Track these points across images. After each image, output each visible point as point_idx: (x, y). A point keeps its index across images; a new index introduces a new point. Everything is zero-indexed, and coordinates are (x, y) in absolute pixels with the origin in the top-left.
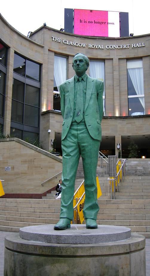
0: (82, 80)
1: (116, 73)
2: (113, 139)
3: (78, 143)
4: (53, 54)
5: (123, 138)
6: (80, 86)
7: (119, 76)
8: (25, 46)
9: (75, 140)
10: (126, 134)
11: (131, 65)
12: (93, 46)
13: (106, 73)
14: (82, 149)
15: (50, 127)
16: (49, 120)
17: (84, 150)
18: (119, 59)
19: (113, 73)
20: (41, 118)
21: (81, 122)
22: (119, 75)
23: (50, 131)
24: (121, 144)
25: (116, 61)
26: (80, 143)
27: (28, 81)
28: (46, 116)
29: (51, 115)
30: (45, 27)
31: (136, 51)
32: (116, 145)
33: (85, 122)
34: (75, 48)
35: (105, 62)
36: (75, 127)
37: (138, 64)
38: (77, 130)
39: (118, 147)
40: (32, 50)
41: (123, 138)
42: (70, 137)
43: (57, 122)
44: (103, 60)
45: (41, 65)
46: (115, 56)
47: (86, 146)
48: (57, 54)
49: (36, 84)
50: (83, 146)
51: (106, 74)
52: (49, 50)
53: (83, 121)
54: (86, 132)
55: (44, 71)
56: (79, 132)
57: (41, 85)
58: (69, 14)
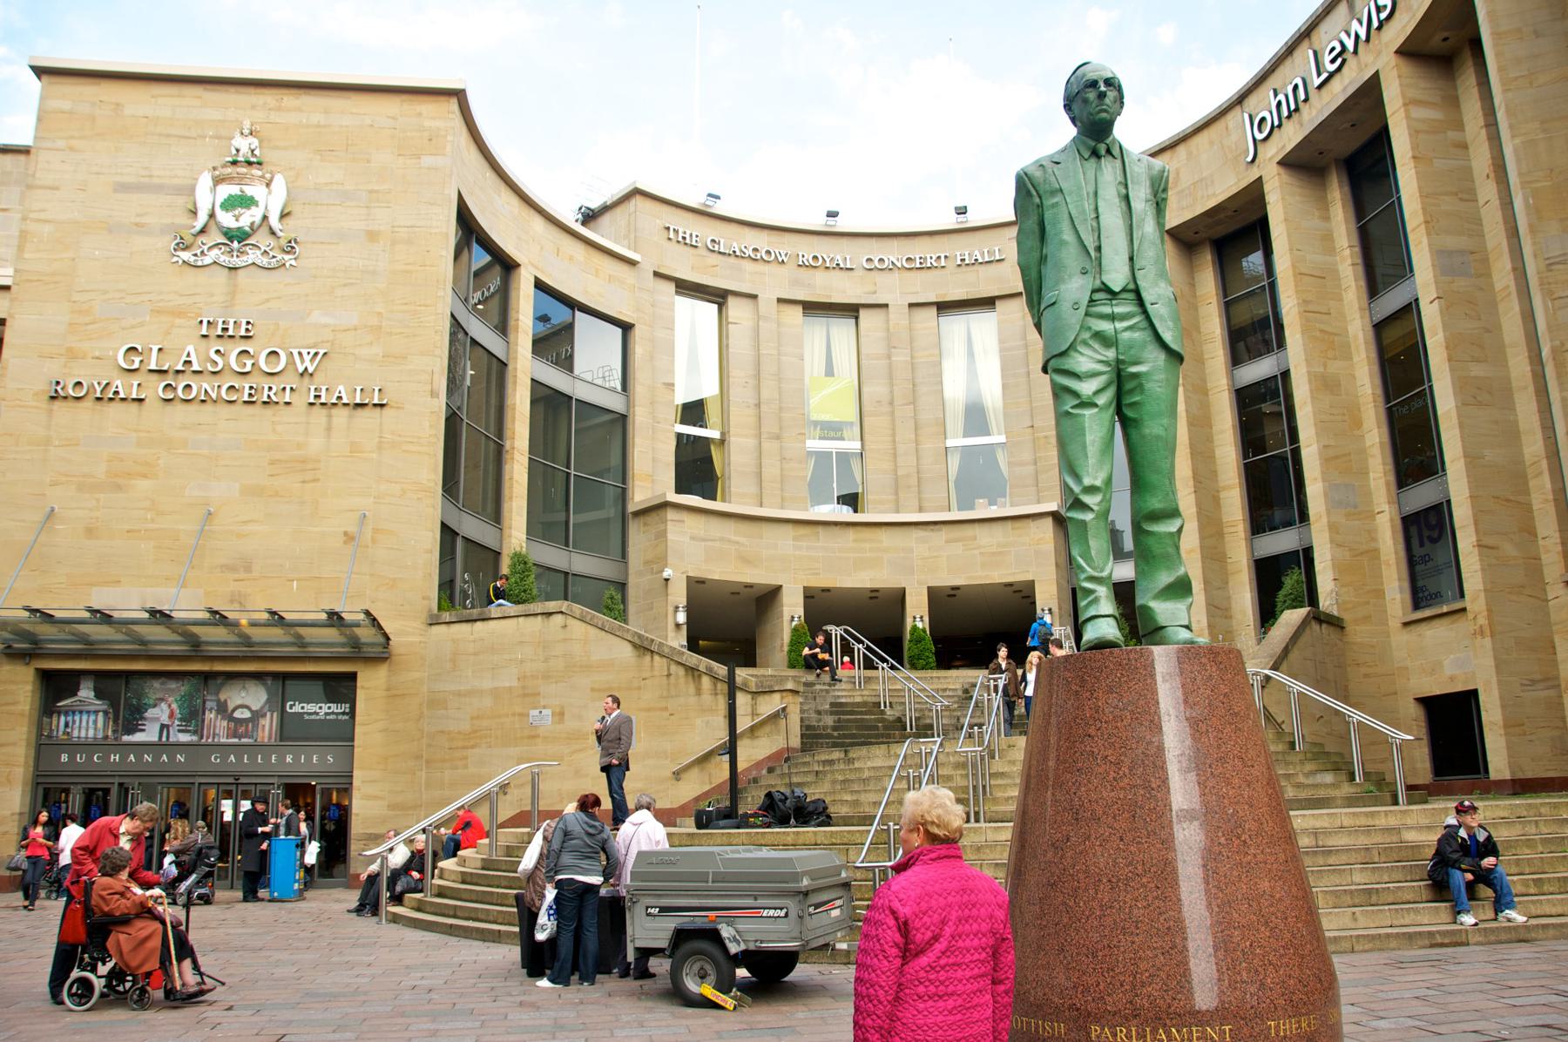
0: (1109, 151)
1: (901, 357)
2: (899, 597)
3: (1118, 361)
4: (671, 287)
5: (933, 593)
6: (1109, 171)
8: (571, 258)
9: (1111, 354)
11: (956, 325)
12: (815, 258)
13: (863, 357)
14: (1128, 386)
15: (670, 560)
16: (665, 531)
17: (1140, 388)
18: (911, 305)
19: (889, 357)
21: (1124, 290)
23: (667, 573)
24: (926, 619)
25: (898, 314)
26: (1123, 362)
28: (653, 518)
29: (671, 514)
31: (970, 275)
33: (1137, 292)
34: (748, 265)
35: (857, 318)
36: (1107, 310)
37: (983, 325)
38: (1112, 318)
40: (597, 276)
41: (933, 593)
42: (1085, 343)
43: (693, 538)
44: (851, 311)
45: (626, 328)
46: (895, 291)
47: (1146, 373)
48: (685, 288)
50: (1136, 376)
51: (863, 362)
52: (656, 274)
53: (1132, 286)
54: (1144, 324)
55: (639, 350)
56: (1120, 325)
57: (629, 403)
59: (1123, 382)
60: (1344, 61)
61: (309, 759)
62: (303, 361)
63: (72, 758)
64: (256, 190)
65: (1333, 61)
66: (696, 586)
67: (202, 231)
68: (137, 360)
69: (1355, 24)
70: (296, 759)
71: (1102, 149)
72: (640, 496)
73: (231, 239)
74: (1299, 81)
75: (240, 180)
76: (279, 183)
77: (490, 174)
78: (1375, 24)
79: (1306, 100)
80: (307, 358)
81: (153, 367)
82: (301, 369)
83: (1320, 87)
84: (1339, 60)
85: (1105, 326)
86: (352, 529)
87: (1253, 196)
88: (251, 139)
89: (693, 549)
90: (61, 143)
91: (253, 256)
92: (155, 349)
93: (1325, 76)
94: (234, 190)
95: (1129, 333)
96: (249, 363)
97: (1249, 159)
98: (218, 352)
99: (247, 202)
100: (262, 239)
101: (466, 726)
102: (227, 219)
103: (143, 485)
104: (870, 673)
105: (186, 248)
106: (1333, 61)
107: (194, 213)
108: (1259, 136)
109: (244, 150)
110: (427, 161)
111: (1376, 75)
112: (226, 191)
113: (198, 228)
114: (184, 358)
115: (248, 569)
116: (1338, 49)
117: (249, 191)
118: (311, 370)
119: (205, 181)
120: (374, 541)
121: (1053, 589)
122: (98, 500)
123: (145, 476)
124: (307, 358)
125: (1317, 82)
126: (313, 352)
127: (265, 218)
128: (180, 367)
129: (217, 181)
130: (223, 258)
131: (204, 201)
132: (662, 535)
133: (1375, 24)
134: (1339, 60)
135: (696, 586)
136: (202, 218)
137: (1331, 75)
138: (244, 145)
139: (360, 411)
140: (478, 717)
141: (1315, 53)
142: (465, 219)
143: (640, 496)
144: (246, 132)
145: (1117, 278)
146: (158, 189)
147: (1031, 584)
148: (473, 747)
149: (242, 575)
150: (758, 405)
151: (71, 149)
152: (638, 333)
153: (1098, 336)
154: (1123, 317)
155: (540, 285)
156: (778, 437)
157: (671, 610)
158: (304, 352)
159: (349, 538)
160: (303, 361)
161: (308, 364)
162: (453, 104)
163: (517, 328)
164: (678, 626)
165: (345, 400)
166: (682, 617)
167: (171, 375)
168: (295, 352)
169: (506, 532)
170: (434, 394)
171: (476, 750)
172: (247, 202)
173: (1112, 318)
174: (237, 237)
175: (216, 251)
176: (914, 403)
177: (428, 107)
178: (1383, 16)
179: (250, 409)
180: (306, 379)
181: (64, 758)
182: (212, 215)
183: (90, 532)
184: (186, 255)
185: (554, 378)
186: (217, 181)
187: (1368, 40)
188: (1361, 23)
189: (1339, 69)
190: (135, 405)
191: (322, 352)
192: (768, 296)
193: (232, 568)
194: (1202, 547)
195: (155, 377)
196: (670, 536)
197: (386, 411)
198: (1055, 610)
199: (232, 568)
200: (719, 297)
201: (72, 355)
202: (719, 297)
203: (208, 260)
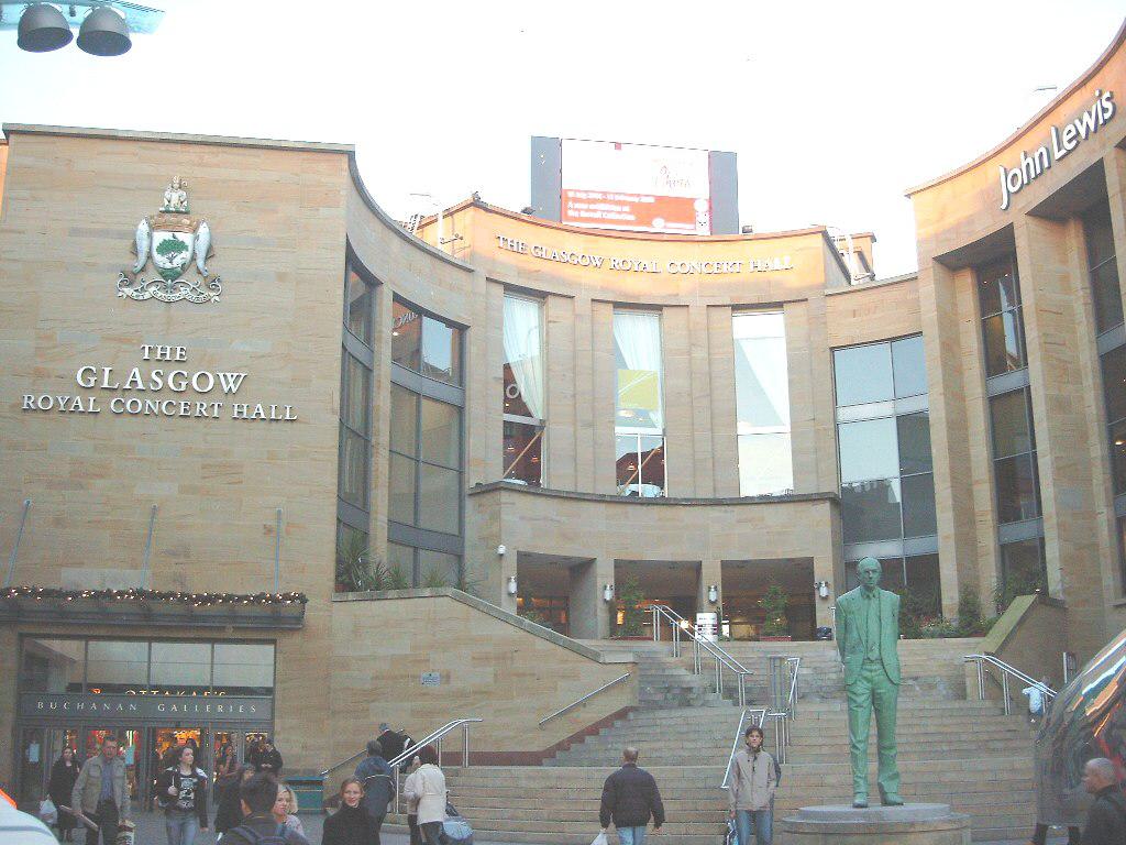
5: (726, 565)
7: (710, 364)
10: (736, 555)
20: (469, 504)
22: (710, 360)
23: (502, 550)
24: (720, 588)
27: (429, 386)
28: (487, 499)
29: (505, 497)
30: (476, 203)
32: (705, 590)
37: (774, 322)
39: (713, 596)
41: (726, 565)
48: (510, 289)
49: (450, 393)
58: (546, 155)
59: (875, 698)
60: (1078, 142)
61: (236, 709)
62: (227, 383)
63: (46, 705)
64: (185, 237)
65: (1070, 141)
66: (524, 558)
67: (143, 270)
68: (93, 380)
69: (1086, 115)
70: (246, 709)
71: (871, 595)
72: (473, 479)
73: (166, 278)
74: (1043, 150)
75: (175, 228)
76: (203, 231)
77: (364, 210)
78: (1101, 122)
79: (1049, 168)
80: (231, 380)
81: (105, 385)
82: (226, 390)
83: (1059, 160)
84: (1074, 142)
85: (867, 674)
86: (272, 523)
87: (1005, 238)
88: (180, 192)
89: (524, 526)
90: (25, 194)
91: (183, 292)
92: (107, 370)
93: (1063, 152)
94: (168, 236)
95: (878, 676)
96: (184, 384)
97: (1004, 207)
98: (158, 373)
99: (178, 246)
100: (190, 278)
101: (368, 687)
102: (161, 260)
103: (99, 483)
104: (685, 644)
105: (130, 284)
106: (1070, 141)
107: (135, 252)
108: (1012, 189)
109: (175, 200)
110: (324, 212)
111: (1101, 161)
112: (161, 236)
113: (139, 268)
114: (131, 378)
115: (187, 555)
116: (1074, 133)
117: (180, 236)
118: (234, 390)
119: (143, 227)
120: (288, 532)
121: (829, 565)
122: (64, 496)
123: (101, 476)
124: (231, 380)
125: (1058, 155)
126: (235, 375)
127: (193, 259)
128: (128, 387)
129: (153, 228)
130: (160, 294)
131: (143, 246)
132: (496, 516)
133: (1101, 122)
134: (1074, 142)
135: (524, 558)
136: (142, 258)
137: (1069, 152)
138: (174, 198)
139: (274, 423)
140: (377, 678)
141: (1057, 130)
142: (352, 261)
143: (473, 479)
144: (176, 186)
145: (874, 655)
146: (105, 233)
147: (811, 560)
148: (373, 701)
149: (182, 560)
150: (574, 396)
151: (35, 199)
152: (470, 335)
153: (866, 678)
154: (876, 671)
155: (397, 298)
156: (591, 425)
157: (504, 580)
158: (229, 375)
159: (268, 530)
160: (227, 383)
161: (231, 385)
162: (345, 159)
163: (381, 337)
164: (510, 594)
165: (263, 416)
166: (513, 587)
167: (119, 392)
168: (221, 375)
169: (373, 516)
170: (334, 413)
171: (377, 704)
172: (178, 246)
173: (871, 671)
174: (172, 276)
175: (153, 288)
176: (710, 395)
177: (322, 165)
178: (1107, 116)
179: (187, 421)
180: (230, 397)
181: (40, 705)
182: (150, 257)
183: (58, 522)
184: (128, 291)
185: (409, 379)
186: (153, 228)
187: (1096, 131)
188: (1090, 114)
189: (1075, 148)
190: (92, 416)
191: (243, 375)
192: (583, 298)
193: (174, 554)
194: (956, 534)
195: (107, 393)
196: (503, 516)
197: (295, 424)
198: (831, 582)
199: (174, 554)
200: (541, 296)
201: (40, 374)
202: (541, 296)
203: (147, 295)
